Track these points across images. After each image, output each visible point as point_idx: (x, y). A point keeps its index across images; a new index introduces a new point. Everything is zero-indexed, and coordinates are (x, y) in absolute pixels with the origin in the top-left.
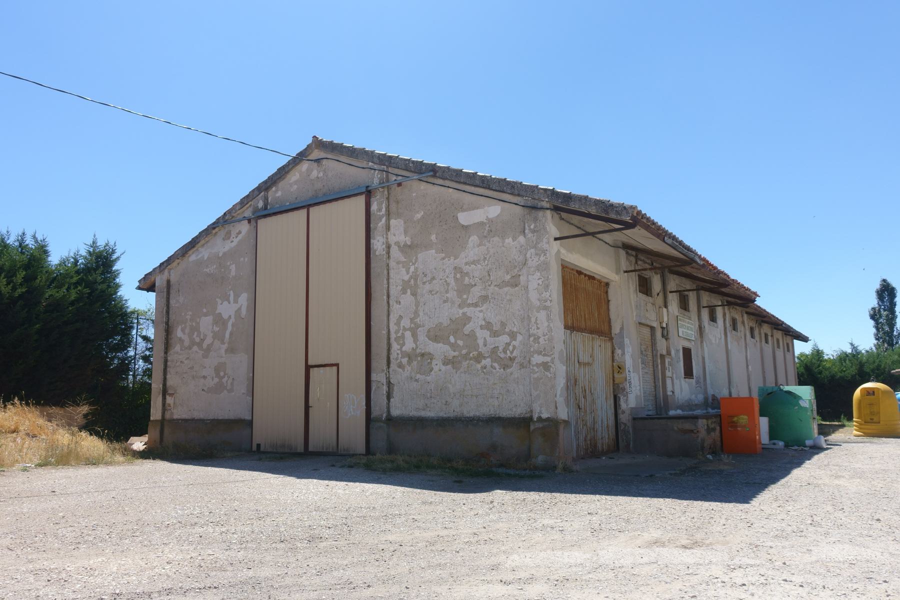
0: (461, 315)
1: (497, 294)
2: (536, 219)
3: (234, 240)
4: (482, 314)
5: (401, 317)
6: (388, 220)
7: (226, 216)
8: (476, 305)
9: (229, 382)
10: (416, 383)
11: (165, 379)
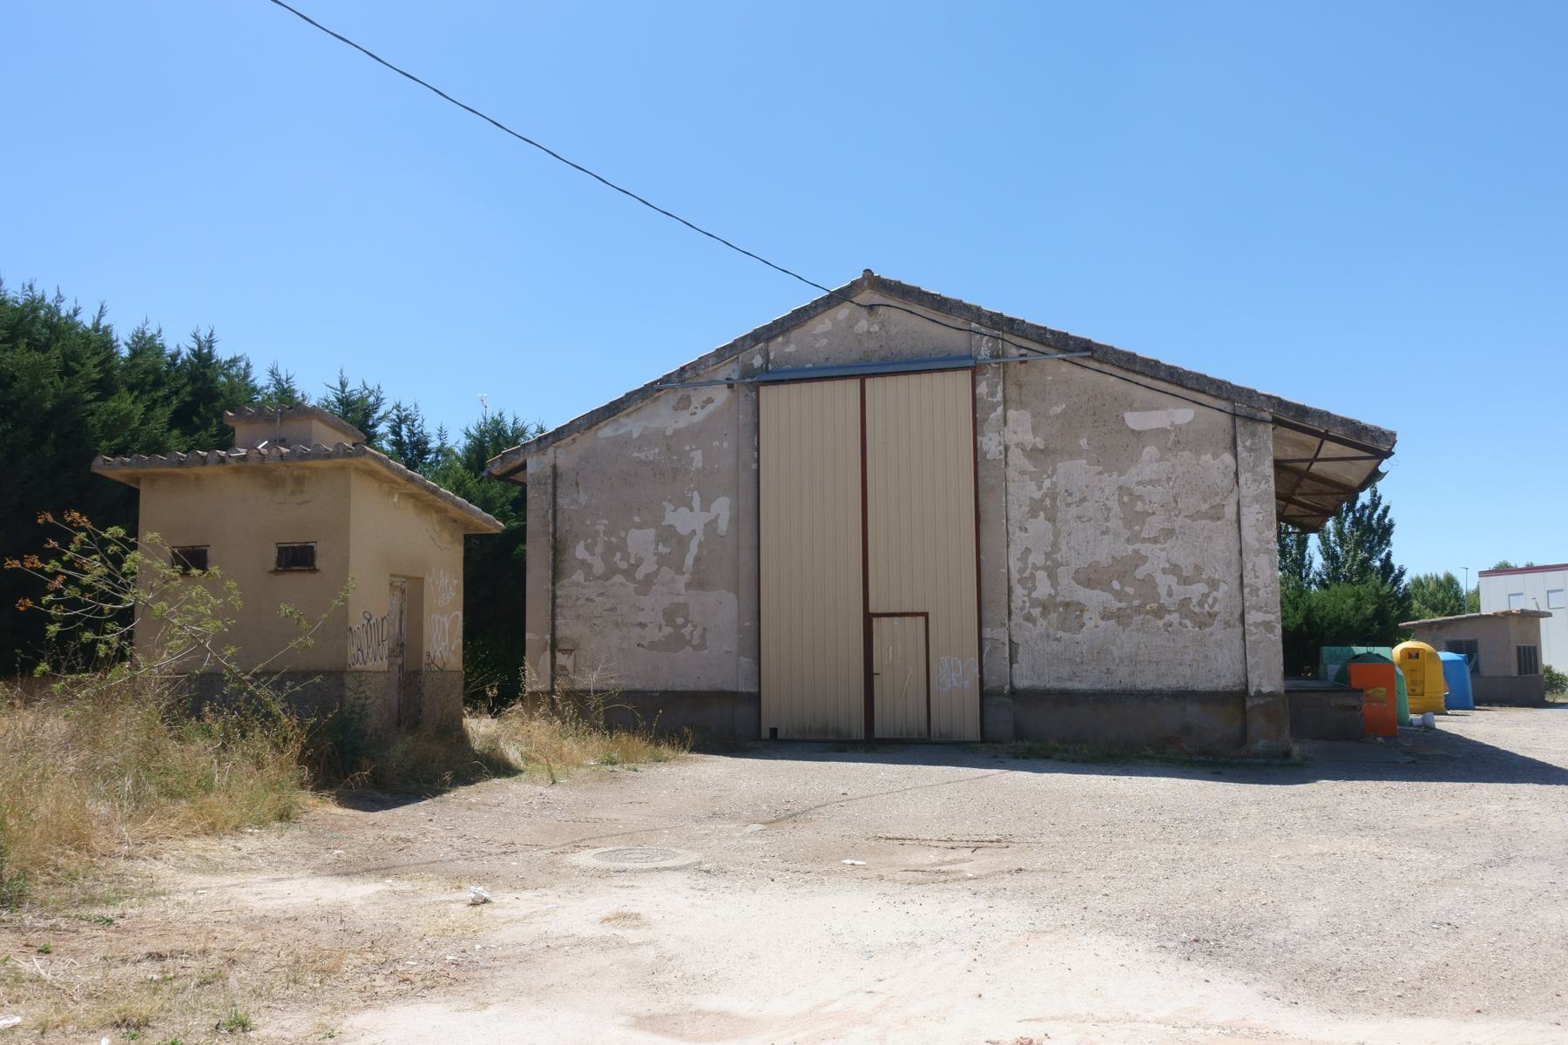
0: (1131, 553)
1: (1189, 529)
2: (1253, 435)
3: (698, 411)
4: (1164, 553)
5: (1028, 551)
6: (1005, 410)
7: (686, 372)
8: (1155, 540)
9: (696, 634)
10: (1056, 643)
11: (554, 627)
